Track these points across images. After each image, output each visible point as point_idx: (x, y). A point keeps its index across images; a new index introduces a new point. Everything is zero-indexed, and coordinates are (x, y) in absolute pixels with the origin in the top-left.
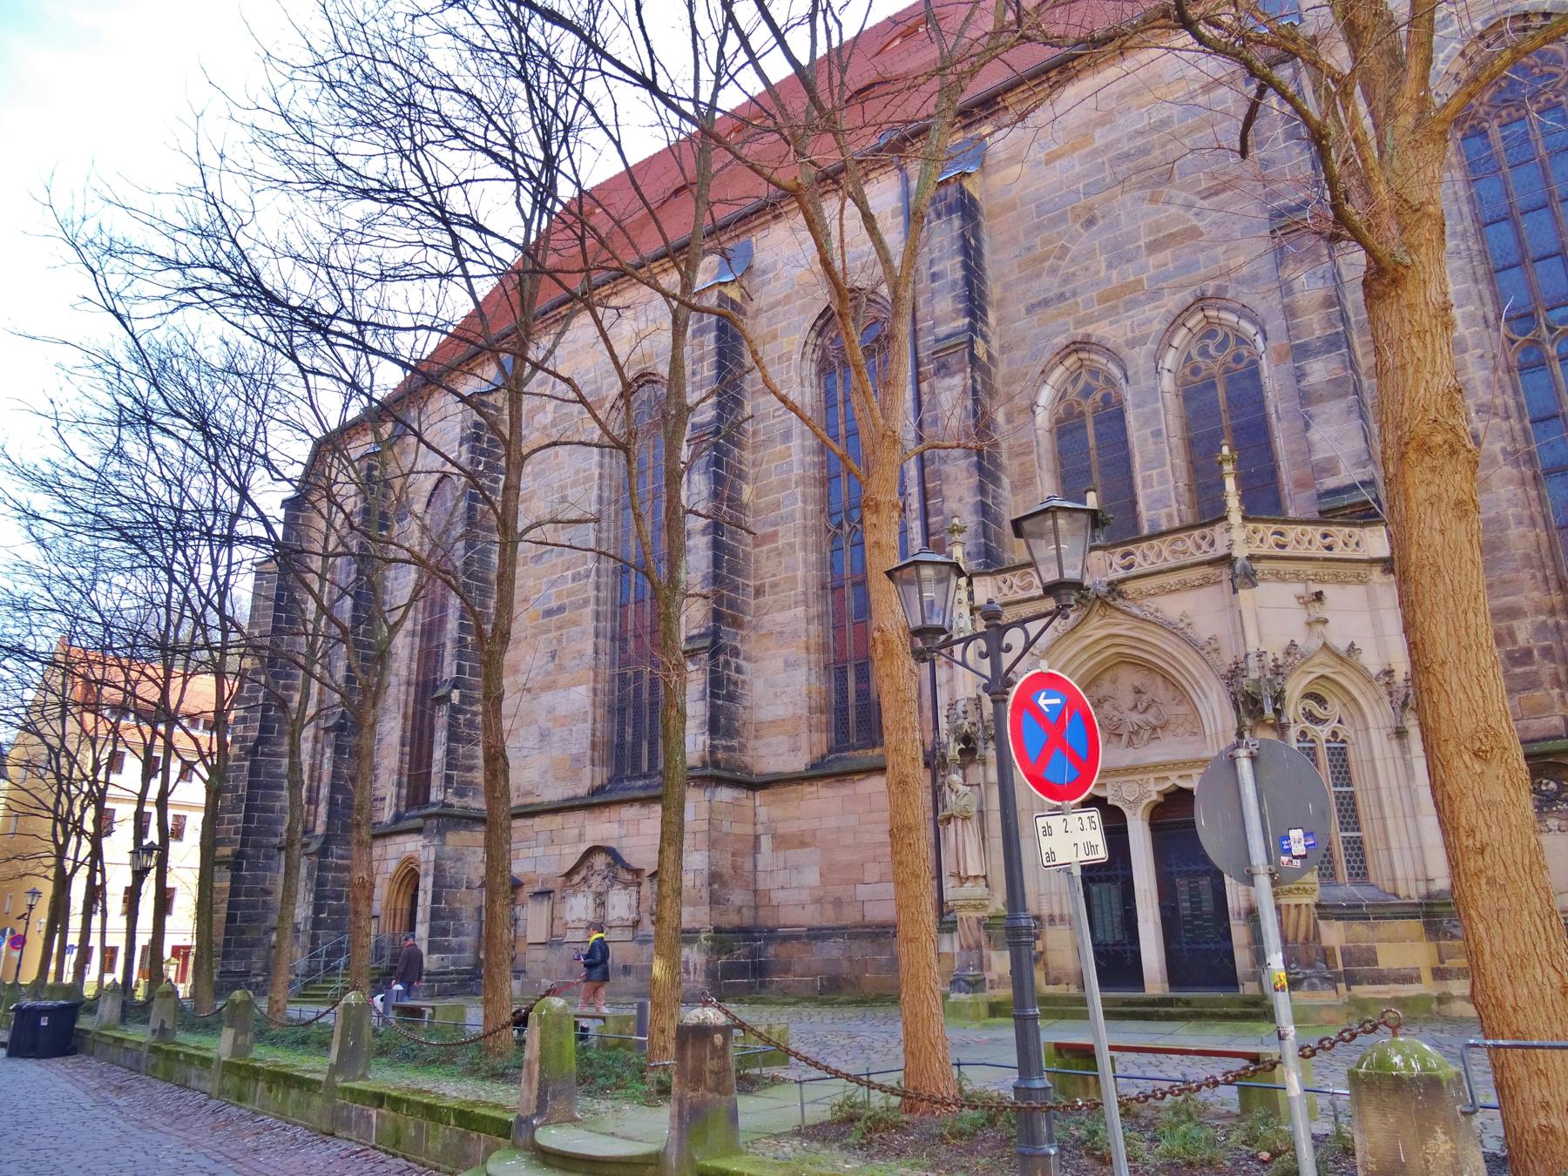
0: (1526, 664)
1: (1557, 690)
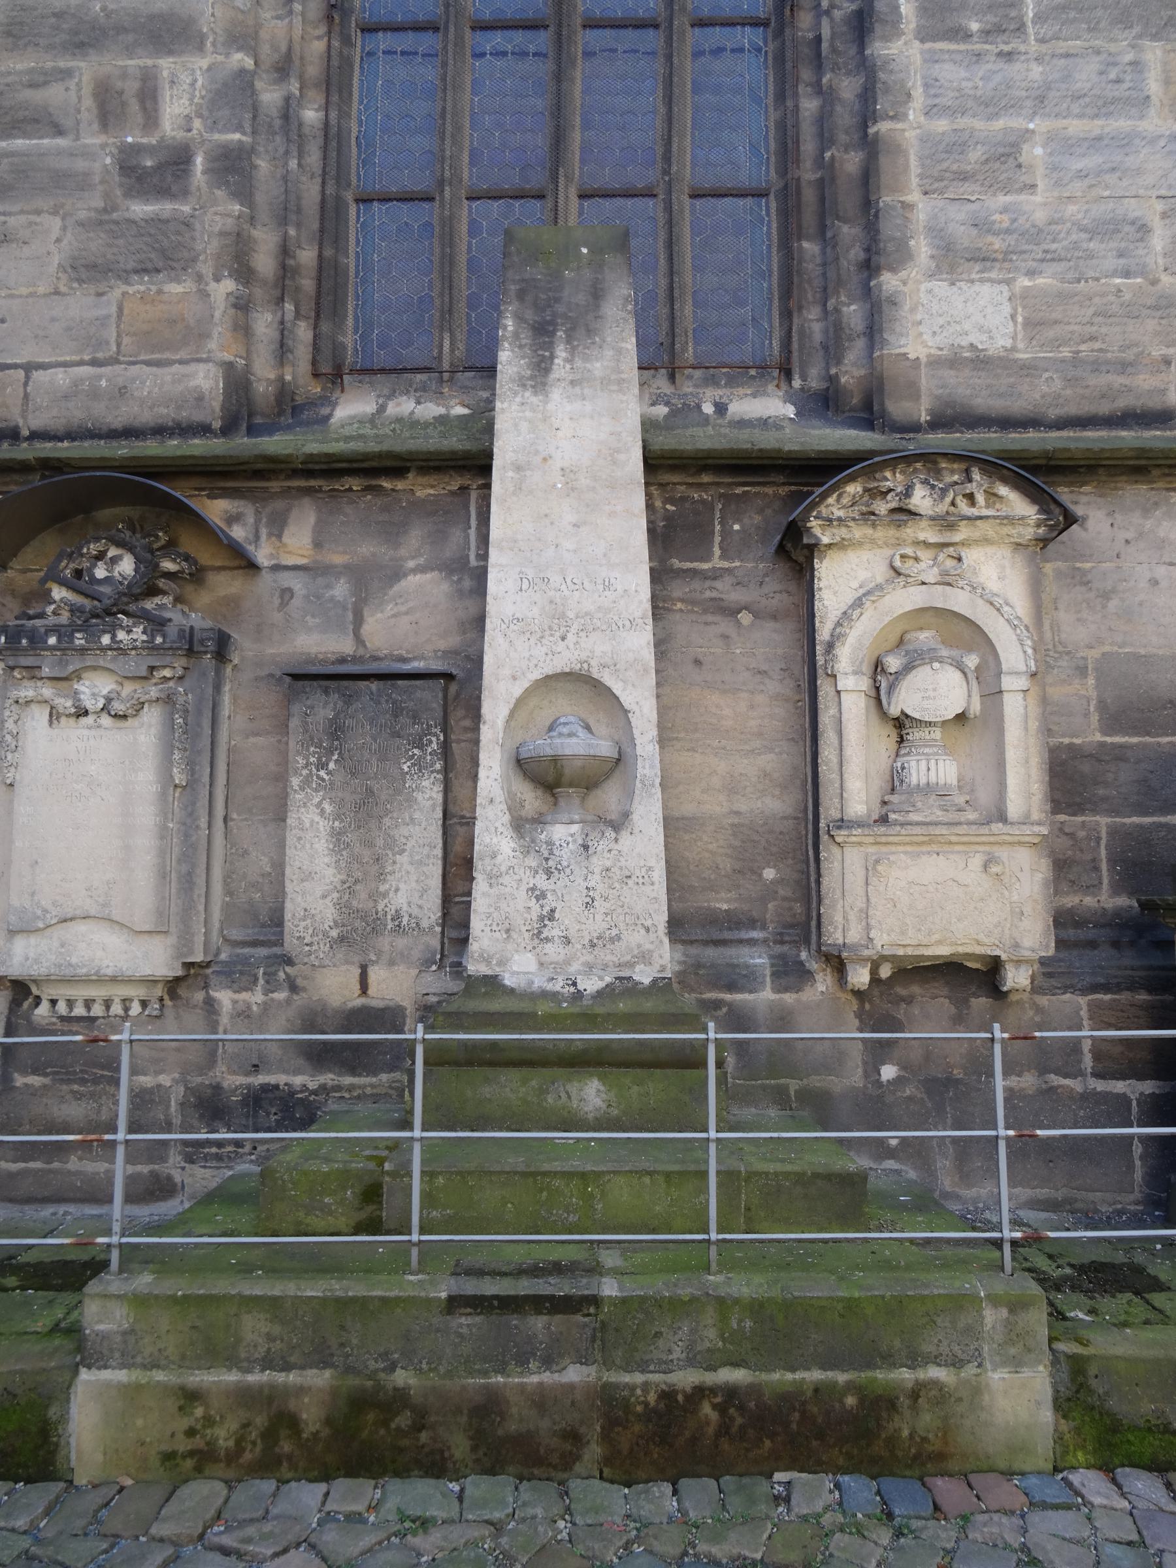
0: (163, 192)
1: (228, 285)
